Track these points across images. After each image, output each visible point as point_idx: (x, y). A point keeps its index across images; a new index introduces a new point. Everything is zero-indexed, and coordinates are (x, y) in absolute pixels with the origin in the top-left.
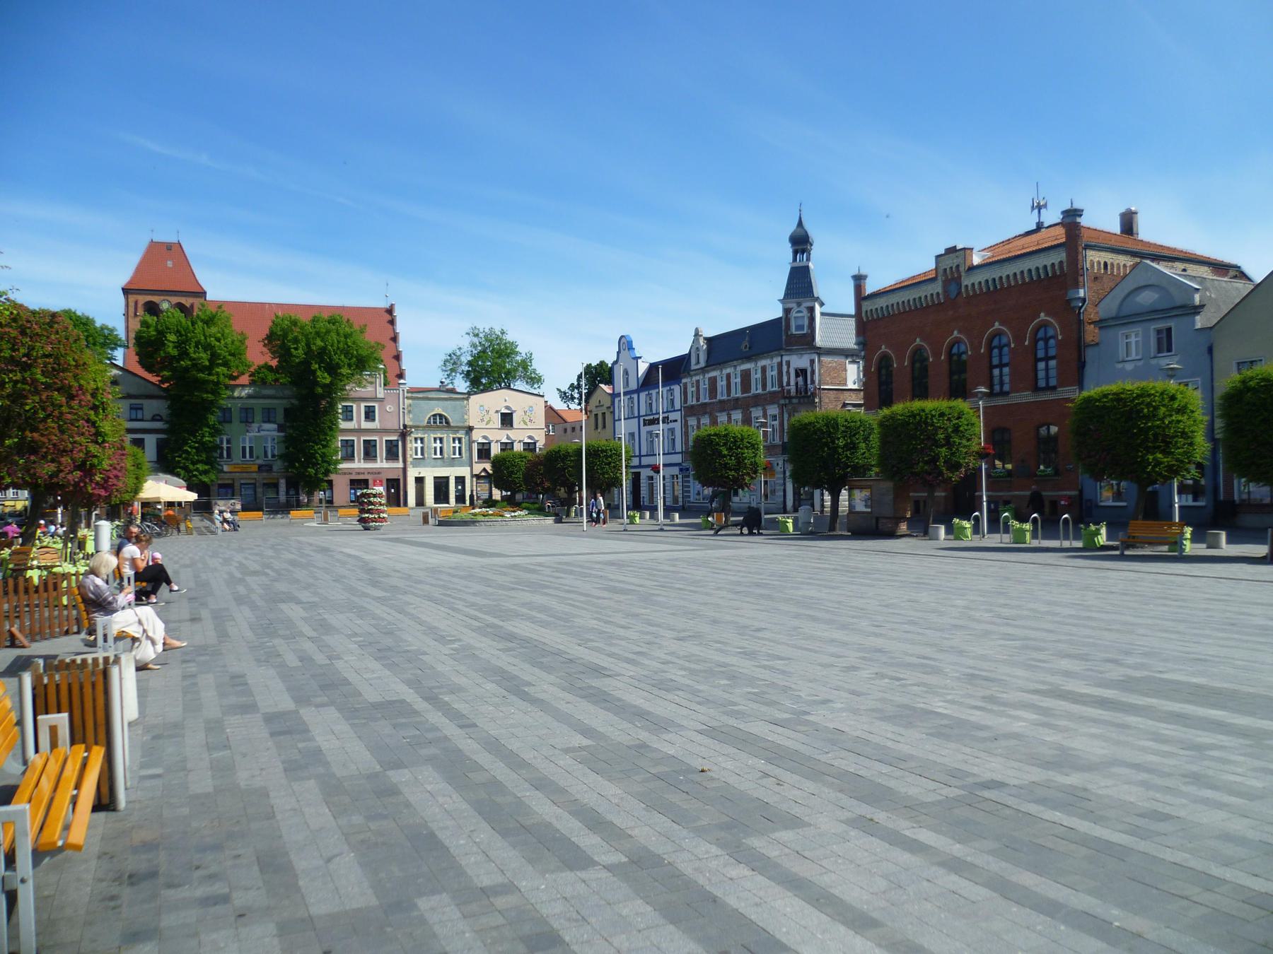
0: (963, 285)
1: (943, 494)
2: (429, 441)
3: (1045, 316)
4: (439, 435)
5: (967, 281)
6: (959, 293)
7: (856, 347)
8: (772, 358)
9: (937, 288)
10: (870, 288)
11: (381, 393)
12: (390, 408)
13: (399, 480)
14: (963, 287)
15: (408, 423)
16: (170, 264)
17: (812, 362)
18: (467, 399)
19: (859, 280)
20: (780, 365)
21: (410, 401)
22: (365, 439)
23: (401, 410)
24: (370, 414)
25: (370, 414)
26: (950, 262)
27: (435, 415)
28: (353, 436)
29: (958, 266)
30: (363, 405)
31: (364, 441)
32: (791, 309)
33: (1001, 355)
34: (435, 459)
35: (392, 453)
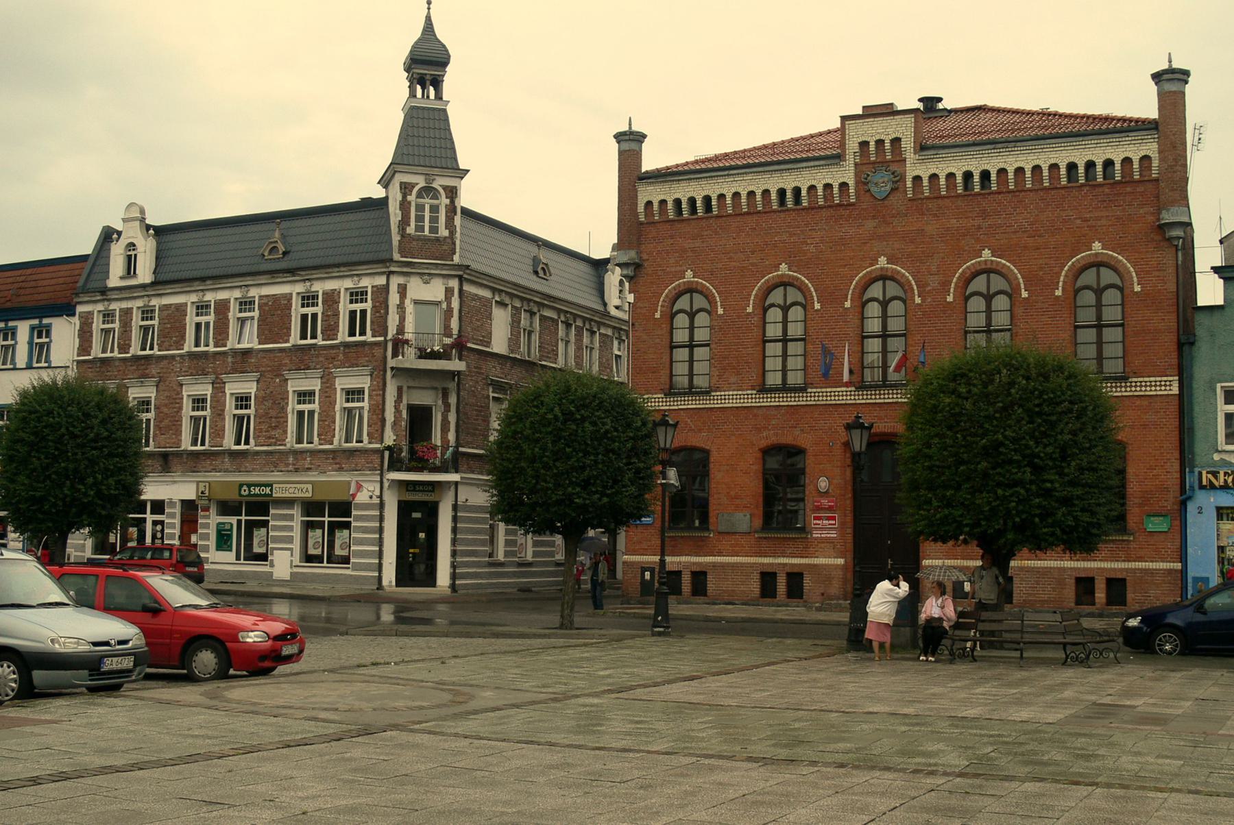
1: (841, 561)
5: (915, 167)
9: (845, 174)
10: (651, 161)
17: (449, 292)
19: (630, 142)
20: (383, 291)
32: (413, 186)
33: (884, 317)
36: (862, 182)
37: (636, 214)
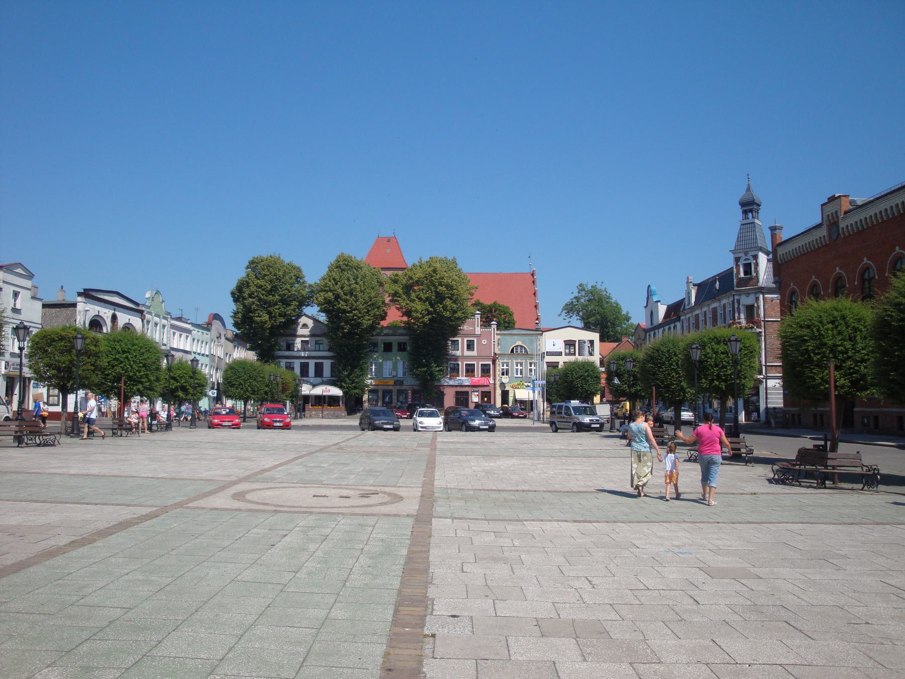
0: (841, 227)
2: (512, 365)
3: (900, 249)
4: (519, 361)
6: (839, 235)
7: (774, 286)
8: (729, 297)
9: (823, 232)
10: (784, 235)
11: (478, 330)
12: (484, 342)
13: (490, 392)
14: (840, 229)
15: (497, 351)
16: (388, 251)
18: (541, 335)
20: (733, 302)
21: (499, 337)
22: (476, 365)
23: (492, 343)
24: (470, 346)
25: (470, 346)
26: (830, 209)
27: (517, 346)
28: (475, 361)
29: (836, 211)
30: (465, 340)
31: (474, 364)
34: (516, 377)
35: (486, 370)
36: (830, 234)
37: (778, 262)
